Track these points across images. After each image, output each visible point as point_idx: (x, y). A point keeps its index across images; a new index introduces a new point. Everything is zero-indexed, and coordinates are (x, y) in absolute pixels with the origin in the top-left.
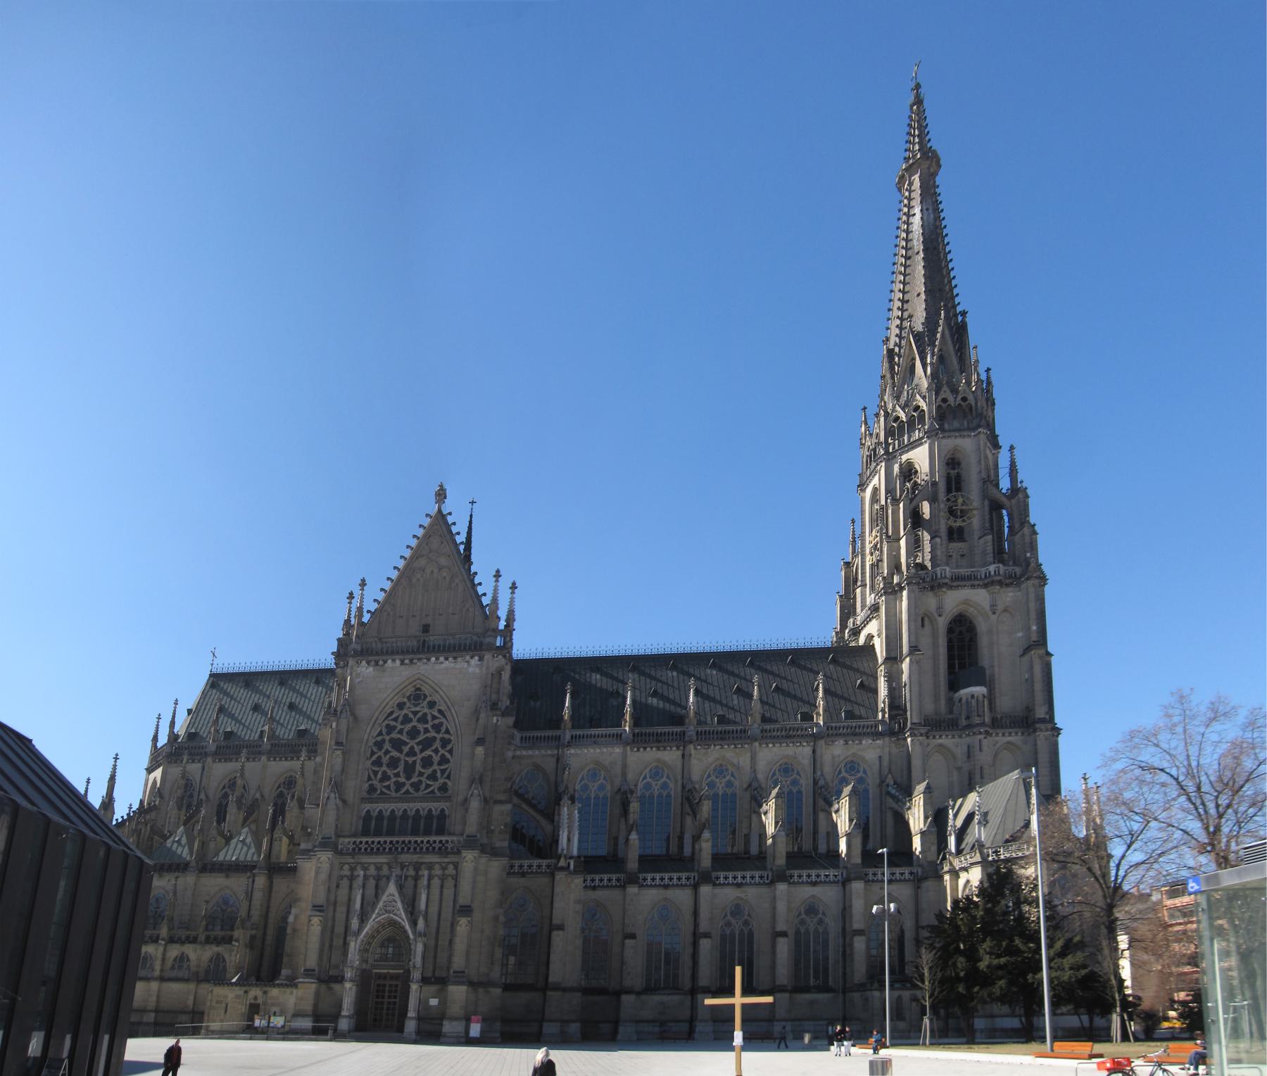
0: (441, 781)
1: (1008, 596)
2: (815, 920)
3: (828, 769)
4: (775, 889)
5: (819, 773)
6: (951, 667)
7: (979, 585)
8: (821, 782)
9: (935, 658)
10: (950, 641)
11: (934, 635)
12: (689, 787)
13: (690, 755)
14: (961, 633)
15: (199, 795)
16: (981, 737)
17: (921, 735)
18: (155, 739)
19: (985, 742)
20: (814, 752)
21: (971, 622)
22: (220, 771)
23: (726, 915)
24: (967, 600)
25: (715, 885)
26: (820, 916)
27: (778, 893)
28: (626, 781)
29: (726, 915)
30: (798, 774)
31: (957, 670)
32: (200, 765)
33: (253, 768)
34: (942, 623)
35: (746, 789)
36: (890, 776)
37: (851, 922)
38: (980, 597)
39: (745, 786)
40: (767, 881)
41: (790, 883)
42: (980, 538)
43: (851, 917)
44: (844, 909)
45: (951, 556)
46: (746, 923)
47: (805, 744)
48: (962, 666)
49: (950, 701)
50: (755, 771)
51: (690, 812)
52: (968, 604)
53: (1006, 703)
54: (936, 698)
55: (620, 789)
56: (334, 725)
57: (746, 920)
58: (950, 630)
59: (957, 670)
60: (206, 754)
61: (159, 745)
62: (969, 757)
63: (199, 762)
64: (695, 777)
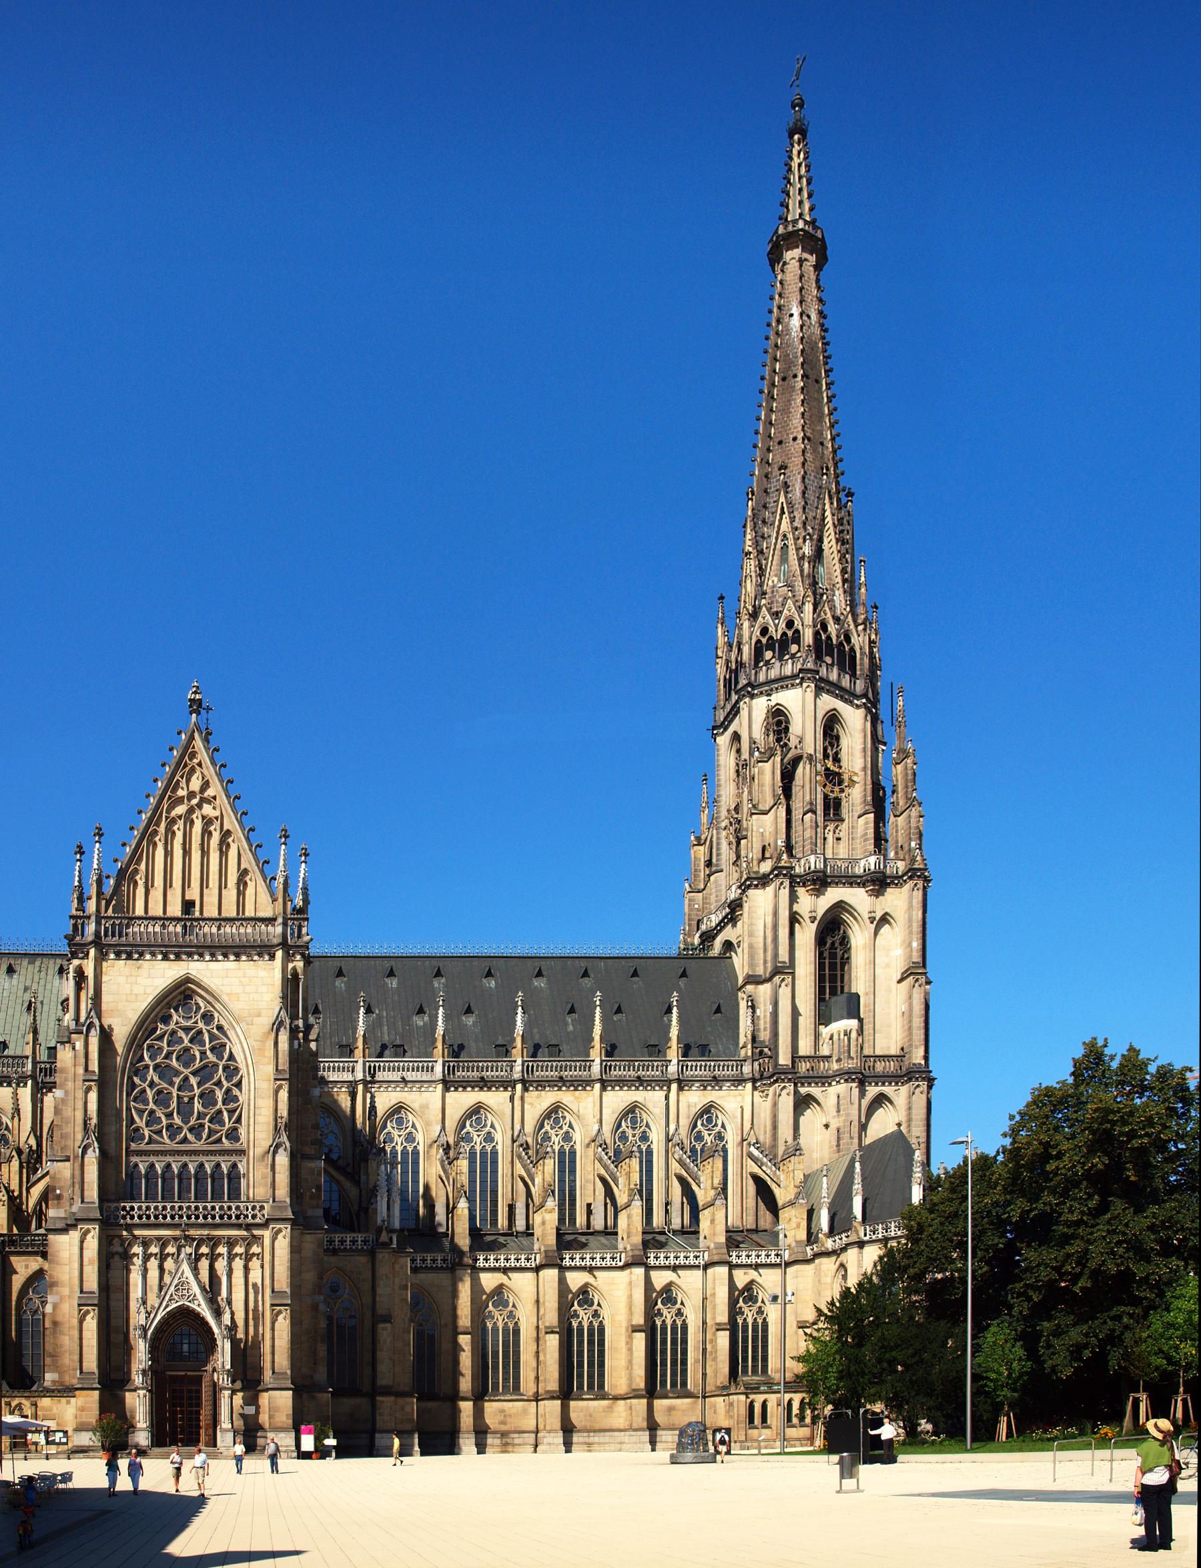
2: (674, 1311)
26: (678, 1306)
31: (827, 996)
37: (714, 1313)
43: (714, 1308)
44: (704, 1299)
46: (596, 1314)
48: (833, 992)
57: (596, 1311)
59: (827, 996)
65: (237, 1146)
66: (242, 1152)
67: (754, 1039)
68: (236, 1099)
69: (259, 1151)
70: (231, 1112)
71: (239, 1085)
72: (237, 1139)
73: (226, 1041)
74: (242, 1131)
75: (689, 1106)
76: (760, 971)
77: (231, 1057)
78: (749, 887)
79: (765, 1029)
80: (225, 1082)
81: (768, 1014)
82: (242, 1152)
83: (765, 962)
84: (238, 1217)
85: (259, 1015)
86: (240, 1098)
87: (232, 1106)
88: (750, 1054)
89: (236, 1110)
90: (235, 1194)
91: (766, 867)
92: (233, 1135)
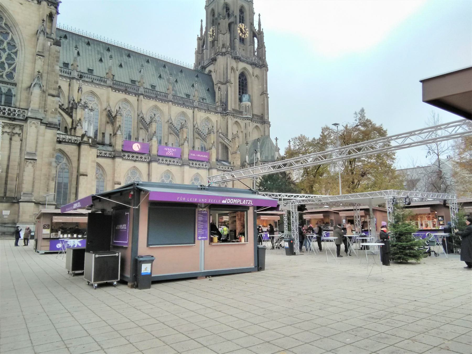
1: (257, 71)
3: (199, 121)
4: (184, 168)
6: (240, 92)
7: (249, 63)
8: (196, 126)
9: (235, 86)
10: (239, 82)
11: (235, 77)
12: (141, 115)
13: (142, 100)
14: (242, 79)
16: (250, 121)
17: (231, 115)
19: (251, 123)
21: (246, 77)
24: (245, 67)
27: (185, 170)
28: (109, 105)
29: (162, 177)
34: (238, 73)
35: (166, 122)
36: (220, 129)
38: (249, 67)
39: (166, 121)
40: (180, 164)
42: (249, 46)
45: (240, 48)
47: (190, 108)
49: (239, 105)
50: (170, 115)
51: (142, 127)
52: (245, 70)
53: (256, 111)
54: (235, 104)
55: (106, 109)
58: (240, 78)
62: (246, 128)
64: (144, 112)
65: (12, 81)
66: (15, 85)
67: (221, 101)
68: (13, 59)
69: (25, 85)
70: (10, 65)
71: (16, 53)
72: (12, 78)
73: (9, 32)
74: (15, 75)
75: (200, 117)
76: (222, 81)
77: (12, 39)
78: (218, 54)
79: (224, 99)
80: (7, 50)
81: (225, 94)
82: (15, 85)
83: (224, 78)
84: (9, 114)
85: (30, 25)
86: (16, 59)
87: (10, 62)
88: (219, 104)
89: (13, 64)
91: (224, 50)
92: (10, 75)
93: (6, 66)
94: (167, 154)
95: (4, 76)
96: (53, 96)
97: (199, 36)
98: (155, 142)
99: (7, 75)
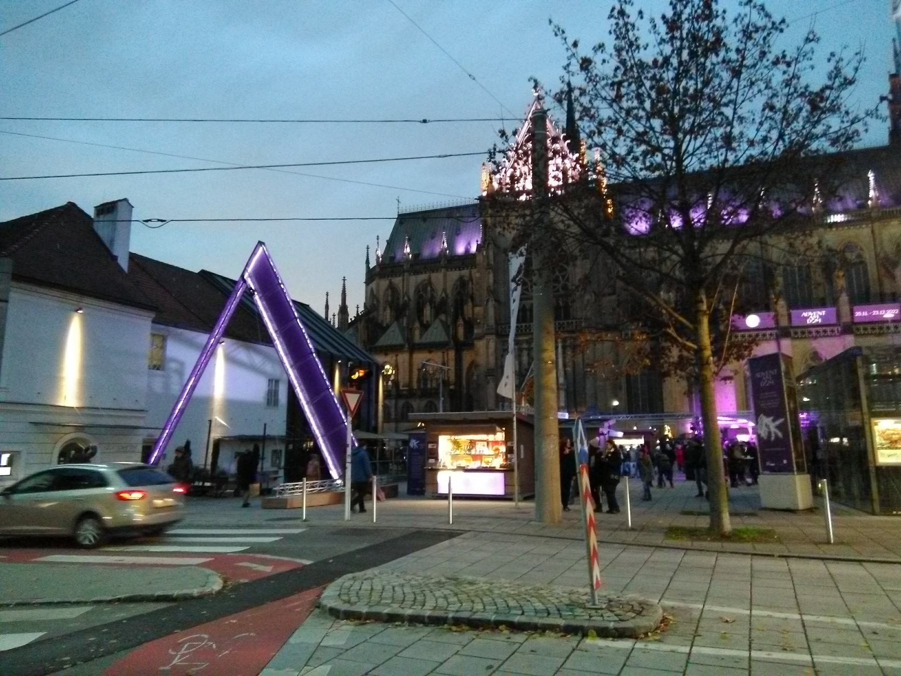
0: (562, 282)
5: (879, 249)
15: (403, 297)
18: (368, 262)
20: (873, 232)
22: (414, 280)
23: (806, 361)
25: (794, 339)
30: (861, 249)
32: (401, 278)
33: (437, 278)
41: (856, 335)
56: (485, 253)
60: (404, 271)
61: (372, 265)
63: (400, 276)
90: (567, 316)
93: (561, 278)
94: (809, 322)
95: (560, 290)
96: (610, 295)
97: (893, 71)
98: (782, 307)
99: (563, 288)
